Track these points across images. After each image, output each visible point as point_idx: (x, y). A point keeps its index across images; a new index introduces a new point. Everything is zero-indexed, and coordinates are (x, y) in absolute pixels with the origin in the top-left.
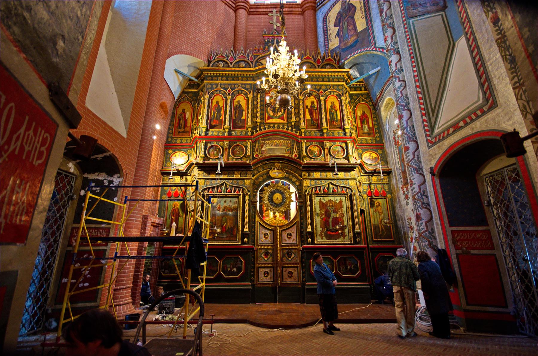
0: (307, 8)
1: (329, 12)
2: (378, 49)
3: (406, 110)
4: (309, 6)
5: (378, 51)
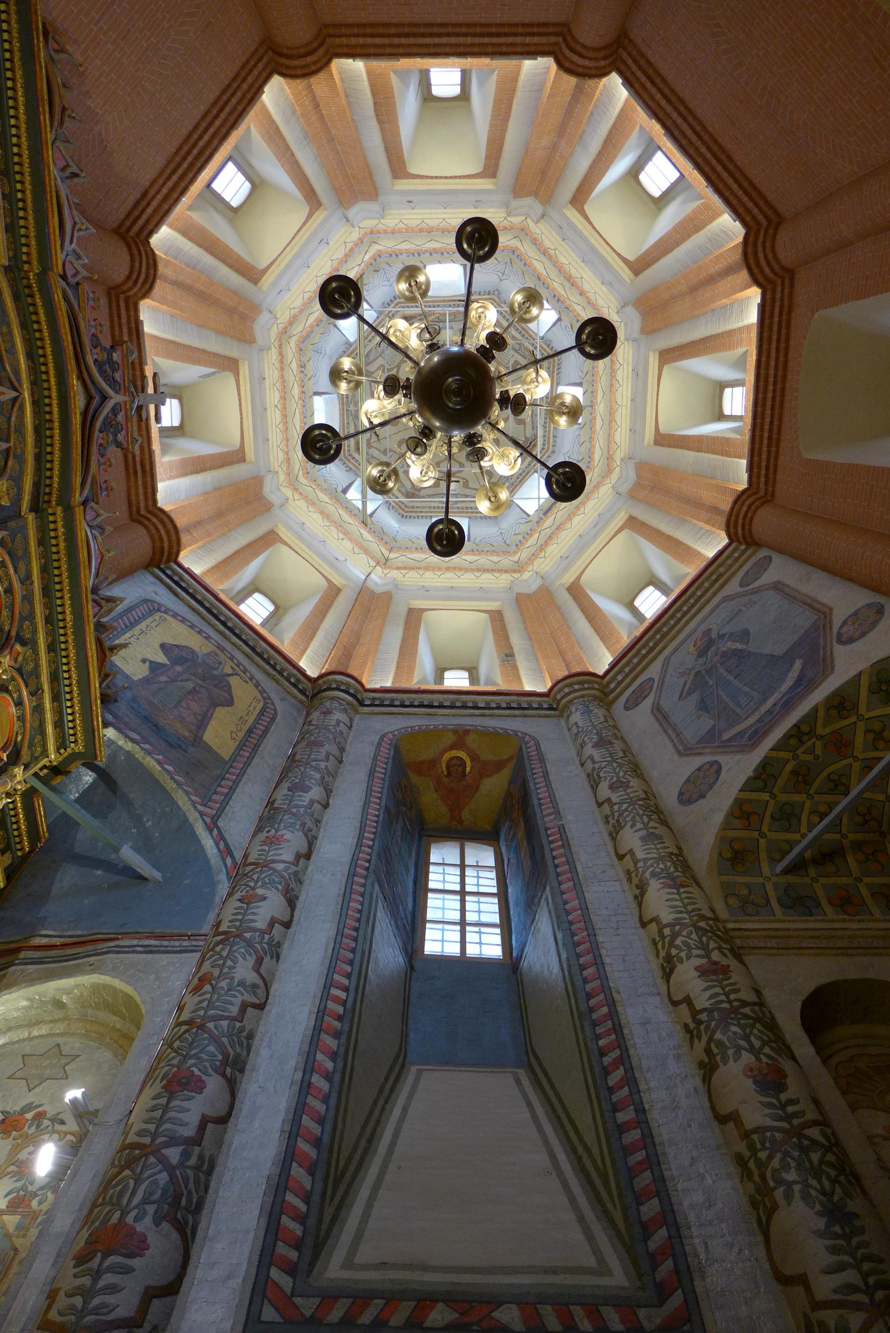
0: (154, 531)
1: (172, 616)
2: (215, 832)
3: (224, 1075)
4: (160, 537)
5: (212, 837)
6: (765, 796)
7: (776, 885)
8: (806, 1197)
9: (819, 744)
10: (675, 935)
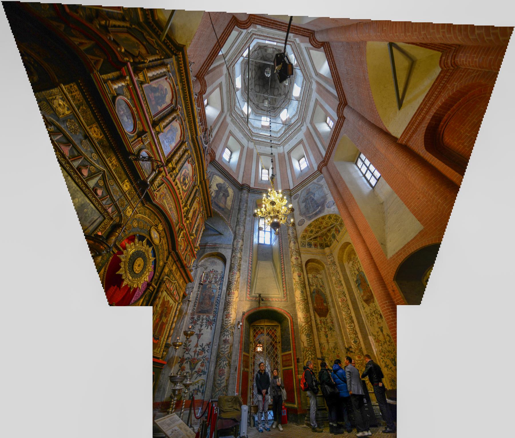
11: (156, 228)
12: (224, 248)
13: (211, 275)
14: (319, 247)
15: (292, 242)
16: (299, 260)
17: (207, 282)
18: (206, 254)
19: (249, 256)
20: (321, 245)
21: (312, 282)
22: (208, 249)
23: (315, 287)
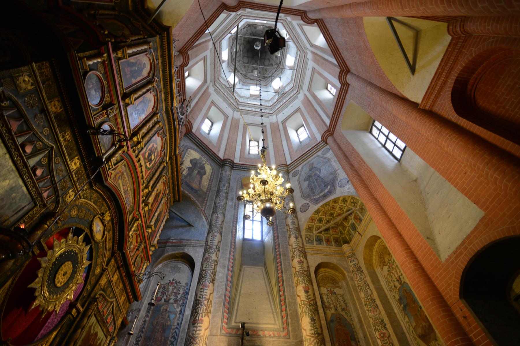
6: (317, 216)
7: (315, 236)
8: (308, 315)
9: (330, 207)
10: (295, 251)
11: (101, 218)
12: (193, 246)
13: (171, 288)
14: (333, 243)
15: (293, 236)
16: (305, 265)
17: (163, 301)
18: (166, 254)
19: (229, 258)
20: (337, 241)
21: (328, 302)
22: (170, 248)
23: (333, 311)
